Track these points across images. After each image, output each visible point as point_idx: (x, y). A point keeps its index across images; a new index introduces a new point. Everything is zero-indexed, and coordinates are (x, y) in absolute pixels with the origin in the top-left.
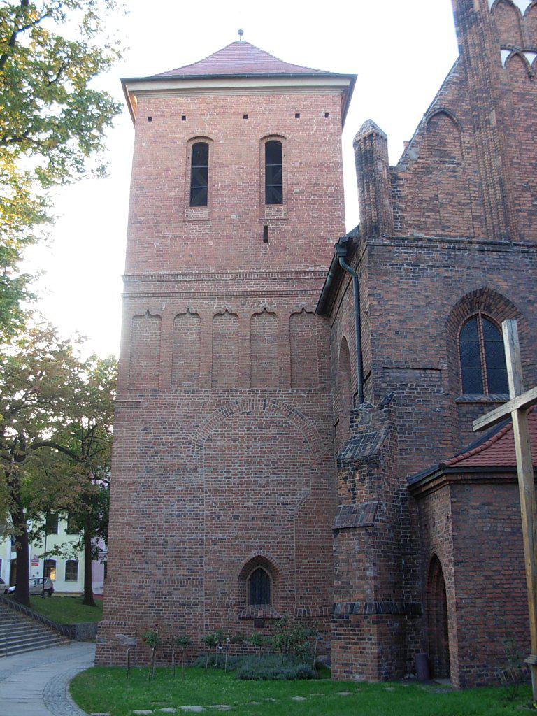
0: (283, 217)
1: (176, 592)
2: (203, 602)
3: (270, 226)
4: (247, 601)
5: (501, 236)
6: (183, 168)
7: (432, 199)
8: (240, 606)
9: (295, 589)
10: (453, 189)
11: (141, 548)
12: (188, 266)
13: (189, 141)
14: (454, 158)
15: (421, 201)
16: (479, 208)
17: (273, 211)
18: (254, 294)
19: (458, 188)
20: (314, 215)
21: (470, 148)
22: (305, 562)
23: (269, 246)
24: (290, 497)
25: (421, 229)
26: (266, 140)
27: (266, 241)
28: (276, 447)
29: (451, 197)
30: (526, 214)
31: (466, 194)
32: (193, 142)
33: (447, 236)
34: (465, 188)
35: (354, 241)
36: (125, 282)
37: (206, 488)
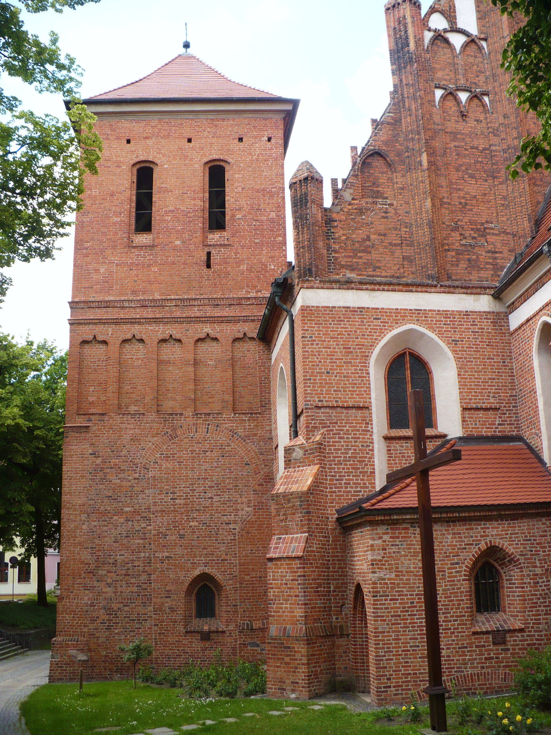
0: (226, 242)
1: (126, 609)
2: (151, 617)
3: (213, 252)
4: (193, 615)
6: (128, 193)
7: (364, 240)
8: (187, 620)
9: (238, 604)
11: (92, 566)
12: (134, 292)
13: (134, 165)
14: (387, 198)
16: (409, 248)
17: (215, 237)
18: (198, 320)
19: (390, 229)
20: (256, 241)
22: (247, 578)
23: (212, 272)
24: (233, 516)
25: (352, 270)
26: (209, 165)
27: (209, 266)
28: (219, 469)
29: (383, 237)
30: (453, 254)
31: (397, 234)
32: (138, 166)
35: (289, 281)
36: (71, 308)
37: (153, 509)
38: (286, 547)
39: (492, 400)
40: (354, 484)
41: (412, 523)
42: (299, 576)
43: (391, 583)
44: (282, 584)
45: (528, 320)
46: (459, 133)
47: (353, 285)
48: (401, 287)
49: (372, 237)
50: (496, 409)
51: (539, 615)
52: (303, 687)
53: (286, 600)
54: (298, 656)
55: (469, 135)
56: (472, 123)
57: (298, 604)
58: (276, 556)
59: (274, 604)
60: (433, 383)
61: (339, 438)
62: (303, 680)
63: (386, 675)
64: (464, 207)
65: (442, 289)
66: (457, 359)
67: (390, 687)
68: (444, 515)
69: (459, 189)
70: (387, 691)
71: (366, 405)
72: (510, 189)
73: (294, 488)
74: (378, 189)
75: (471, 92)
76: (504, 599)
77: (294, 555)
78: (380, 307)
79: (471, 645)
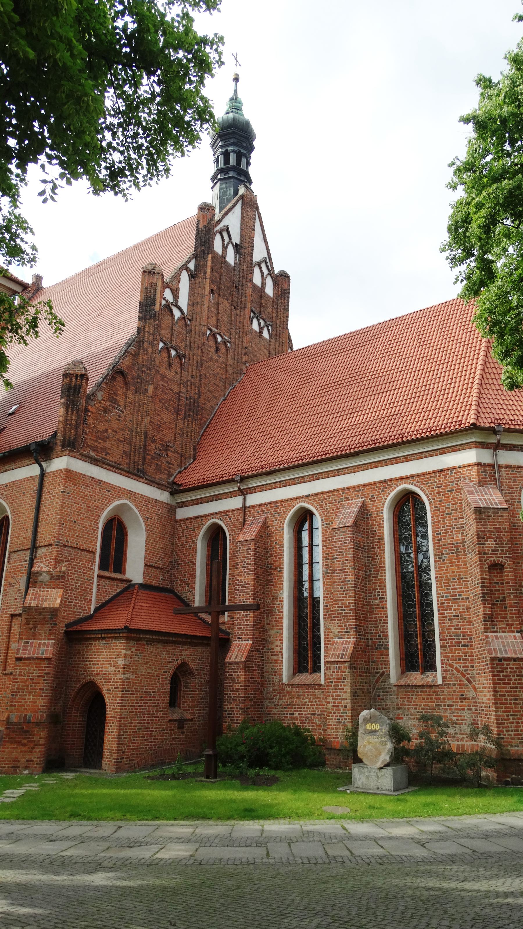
5: (138, 470)
10: (117, 428)
14: (120, 406)
15: (98, 431)
19: (119, 429)
21: (131, 403)
25: (94, 450)
30: (150, 457)
33: (107, 460)
34: (123, 430)
35: (51, 445)
38: (34, 650)
39: (160, 562)
40: (79, 606)
41: (147, 641)
42: (46, 674)
43: (133, 683)
44: (27, 679)
45: (197, 517)
46: (166, 377)
48: (124, 473)
49: (109, 431)
50: (161, 569)
51: (200, 710)
52: (37, 764)
53: (30, 693)
54: (36, 738)
56: (173, 373)
57: (42, 696)
58: (27, 656)
59: (17, 695)
60: (127, 543)
61: (75, 571)
62: (38, 758)
63: (122, 750)
64: (159, 428)
65: (146, 481)
66: (147, 530)
67: (123, 758)
68: (165, 638)
69: (159, 415)
70: (121, 762)
71: (94, 550)
73: (46, 604)
75: (177, 352)
76: (180, 699)
77: (44, 656)
78: (111, 483)
79: (167, 728)
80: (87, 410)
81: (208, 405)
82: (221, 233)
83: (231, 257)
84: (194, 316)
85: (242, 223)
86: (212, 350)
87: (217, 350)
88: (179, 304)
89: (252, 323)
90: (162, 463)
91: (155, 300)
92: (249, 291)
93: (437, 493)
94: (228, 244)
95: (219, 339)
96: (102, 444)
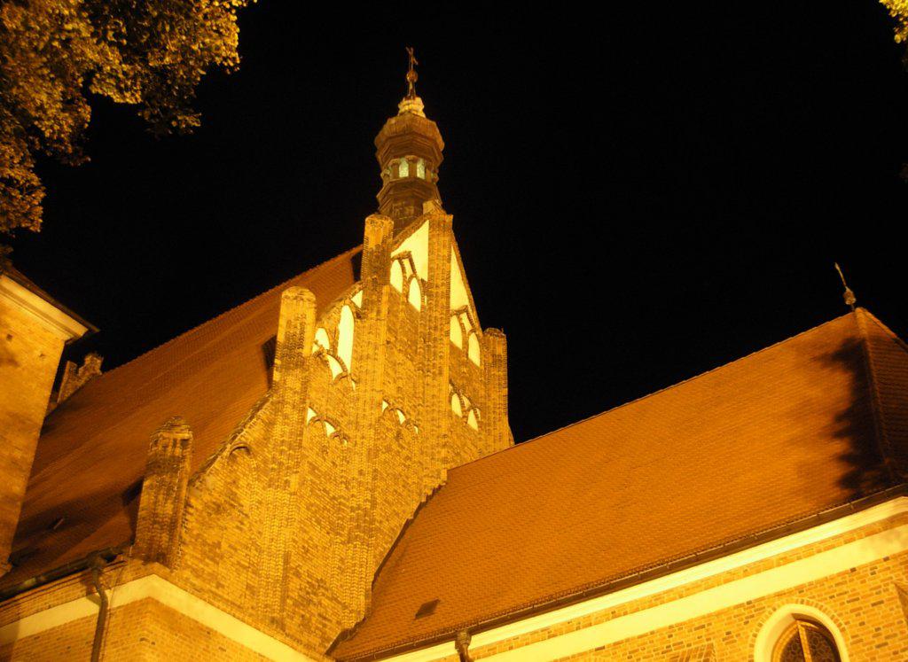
15: (204, 543)
16: (254, 576)
19: (241, 544)
25: (198, 577)
29: (232, 551)
46: (318, 469)
47: (206, 596)
49: (224, 546)
55: (326, 474)
69: (305, 531)
72: (350, 553)
74: (237, 492)
80: (188, 505)
81: (386, 524)
82: (400, 259)
83: (416, 299)
84: (363, 377)
85: (431, 252)
86: (390, 435)
87: (399, 436)
88: (340, 354)
89: (450, 401)
90: (312, 614)
91: (302, 339)
92: (446, 350)
93: (852, 611)
94: (411, 277)
95: (402, 418)
96: (210, 567)
